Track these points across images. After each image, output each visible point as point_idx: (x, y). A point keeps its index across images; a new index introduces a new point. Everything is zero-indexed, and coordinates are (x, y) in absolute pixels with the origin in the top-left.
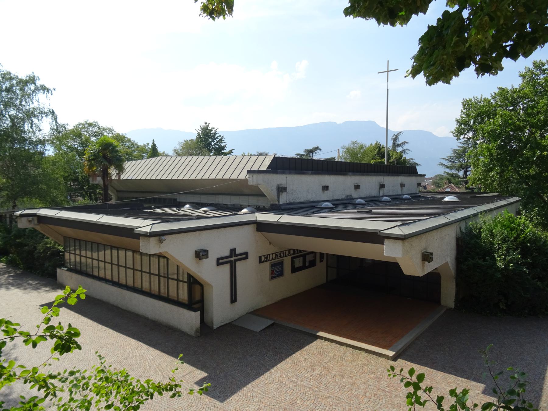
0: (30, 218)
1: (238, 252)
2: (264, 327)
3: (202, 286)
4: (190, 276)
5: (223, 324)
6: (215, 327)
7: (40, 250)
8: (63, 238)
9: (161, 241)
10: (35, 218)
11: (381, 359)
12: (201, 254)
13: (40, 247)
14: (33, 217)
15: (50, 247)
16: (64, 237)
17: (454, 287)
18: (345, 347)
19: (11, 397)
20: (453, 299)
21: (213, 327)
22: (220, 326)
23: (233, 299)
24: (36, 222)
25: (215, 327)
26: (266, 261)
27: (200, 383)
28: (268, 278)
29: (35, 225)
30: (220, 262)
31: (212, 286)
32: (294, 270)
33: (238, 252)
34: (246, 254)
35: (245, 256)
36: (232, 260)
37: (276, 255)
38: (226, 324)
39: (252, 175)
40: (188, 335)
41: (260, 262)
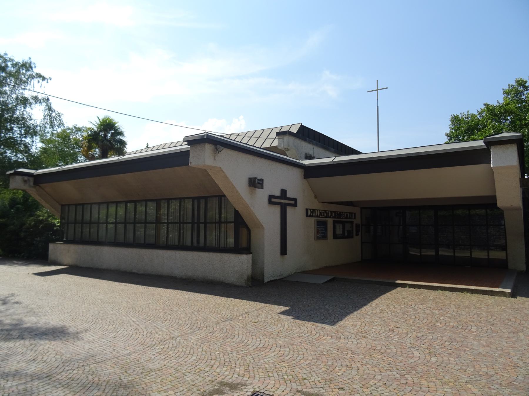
0: (26, 178)
1: (288, 195)
2: (326, 280)
3: (249, 230)
4: (237, 213)
5: (273, 279)
6: (266, 280)
7: (30, 224)
8: (59, 207)
9: (217, 151)
10: (32, 179)
11: (497, 297)
12: (255, 183)
13: (30, 221)
14: (29, 178)
15: (42, 220)
16: (62, 206)
17: (524, 246)
18: (440, 292)
19: (22, 326)
20: (524, 260)
21: (263, 280)
22: (271, 281)
23: (283, 251)
24: (32, 183)
25: (266, 280)
26: (312, 216)
27: (526, 83)
28: (313, 238)
29: (30, 186)
30: (271, 200)
31: (263, 228)
32: (335, 237)
33: (288, 195)
34: (295, 200)
35: (294, 203)
36: (282, 202)
37: (320, 213)
38: (276, 280)
39: (281, 137)
40: (235, 286)
41: (307, 215)
